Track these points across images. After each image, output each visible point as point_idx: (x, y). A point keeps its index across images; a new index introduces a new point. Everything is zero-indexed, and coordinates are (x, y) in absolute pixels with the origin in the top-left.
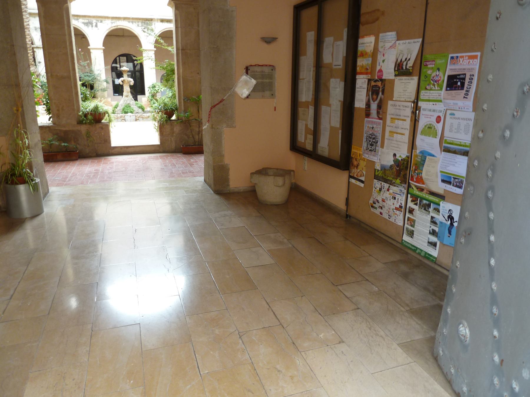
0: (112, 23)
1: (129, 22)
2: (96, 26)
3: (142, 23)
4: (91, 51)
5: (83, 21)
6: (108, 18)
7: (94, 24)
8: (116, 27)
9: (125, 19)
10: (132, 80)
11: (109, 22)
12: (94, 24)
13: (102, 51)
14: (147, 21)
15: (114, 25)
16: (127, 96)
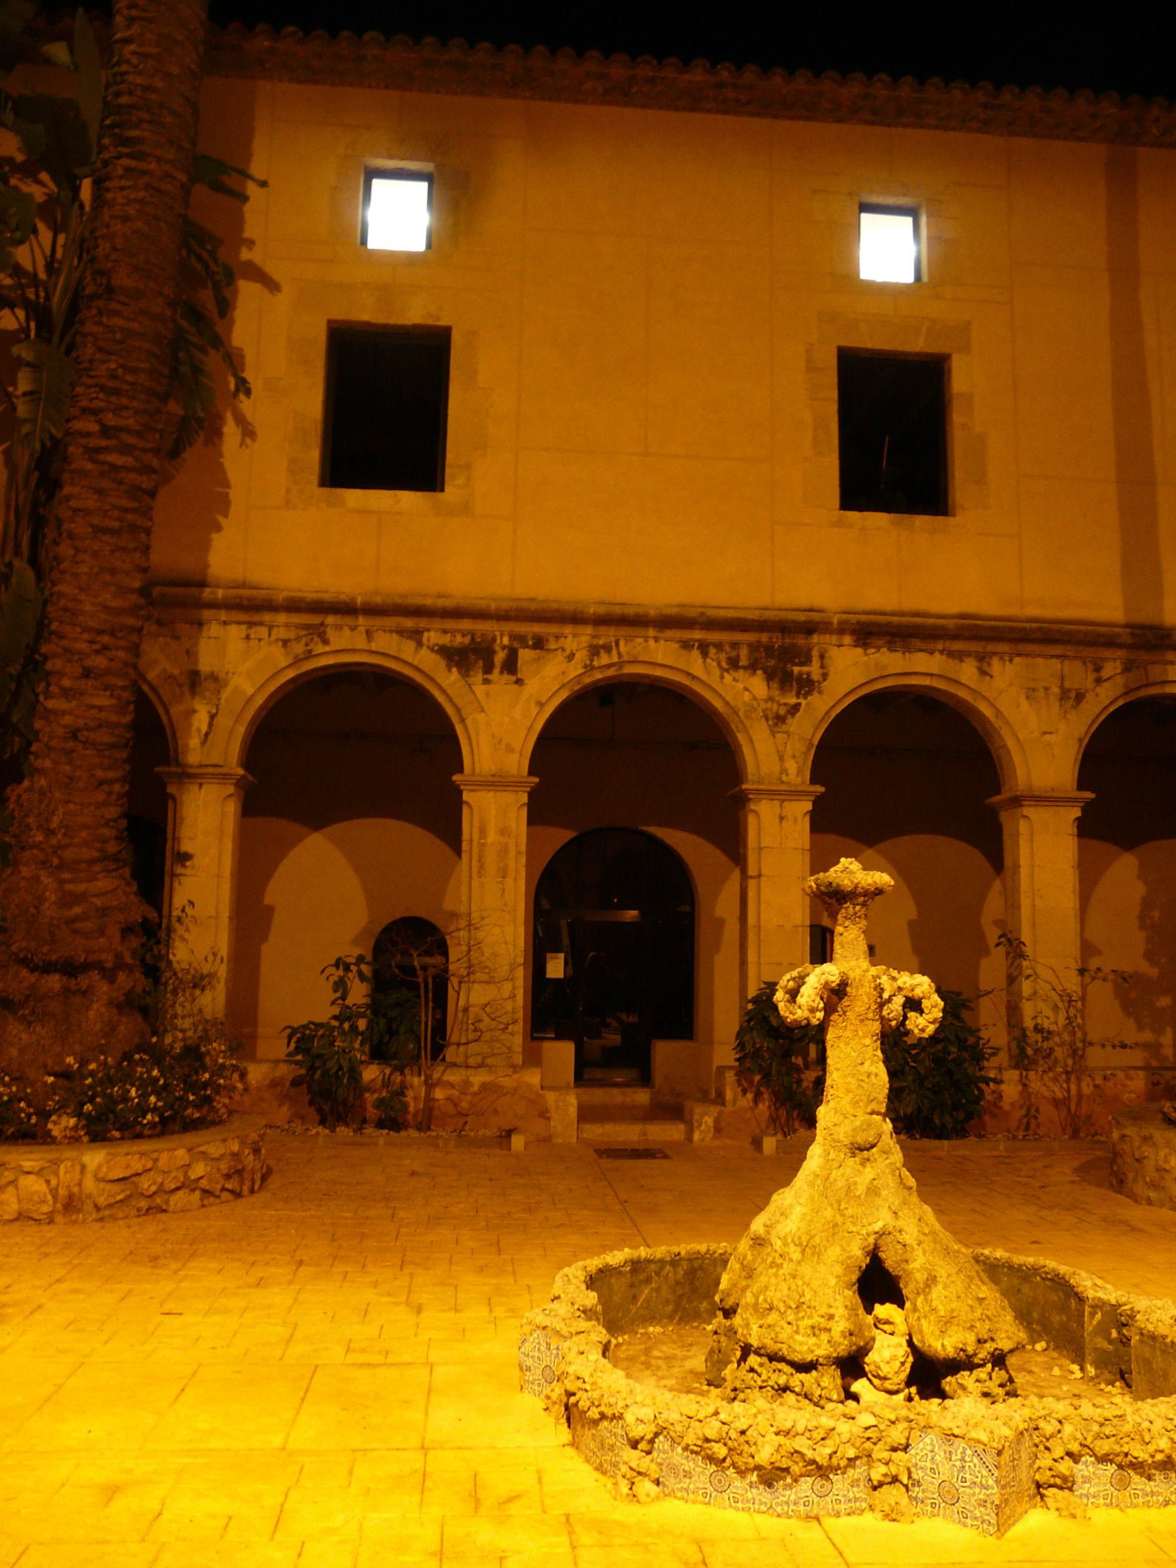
0: (594, 651)
1: (686, 645)
2: (510, 666)
3: (754, 647)
4: (466, 796)
5: (445, 640)
6: (574, 618)
7: (500, 657)
8: (611, 672)
9: (667, 622)
10: (922, 984)
11: (577, 640)
12: (500, 657)
13: (524, 798)
14: (781, 646)
15: (604, 659)
16: (861, 1149)
